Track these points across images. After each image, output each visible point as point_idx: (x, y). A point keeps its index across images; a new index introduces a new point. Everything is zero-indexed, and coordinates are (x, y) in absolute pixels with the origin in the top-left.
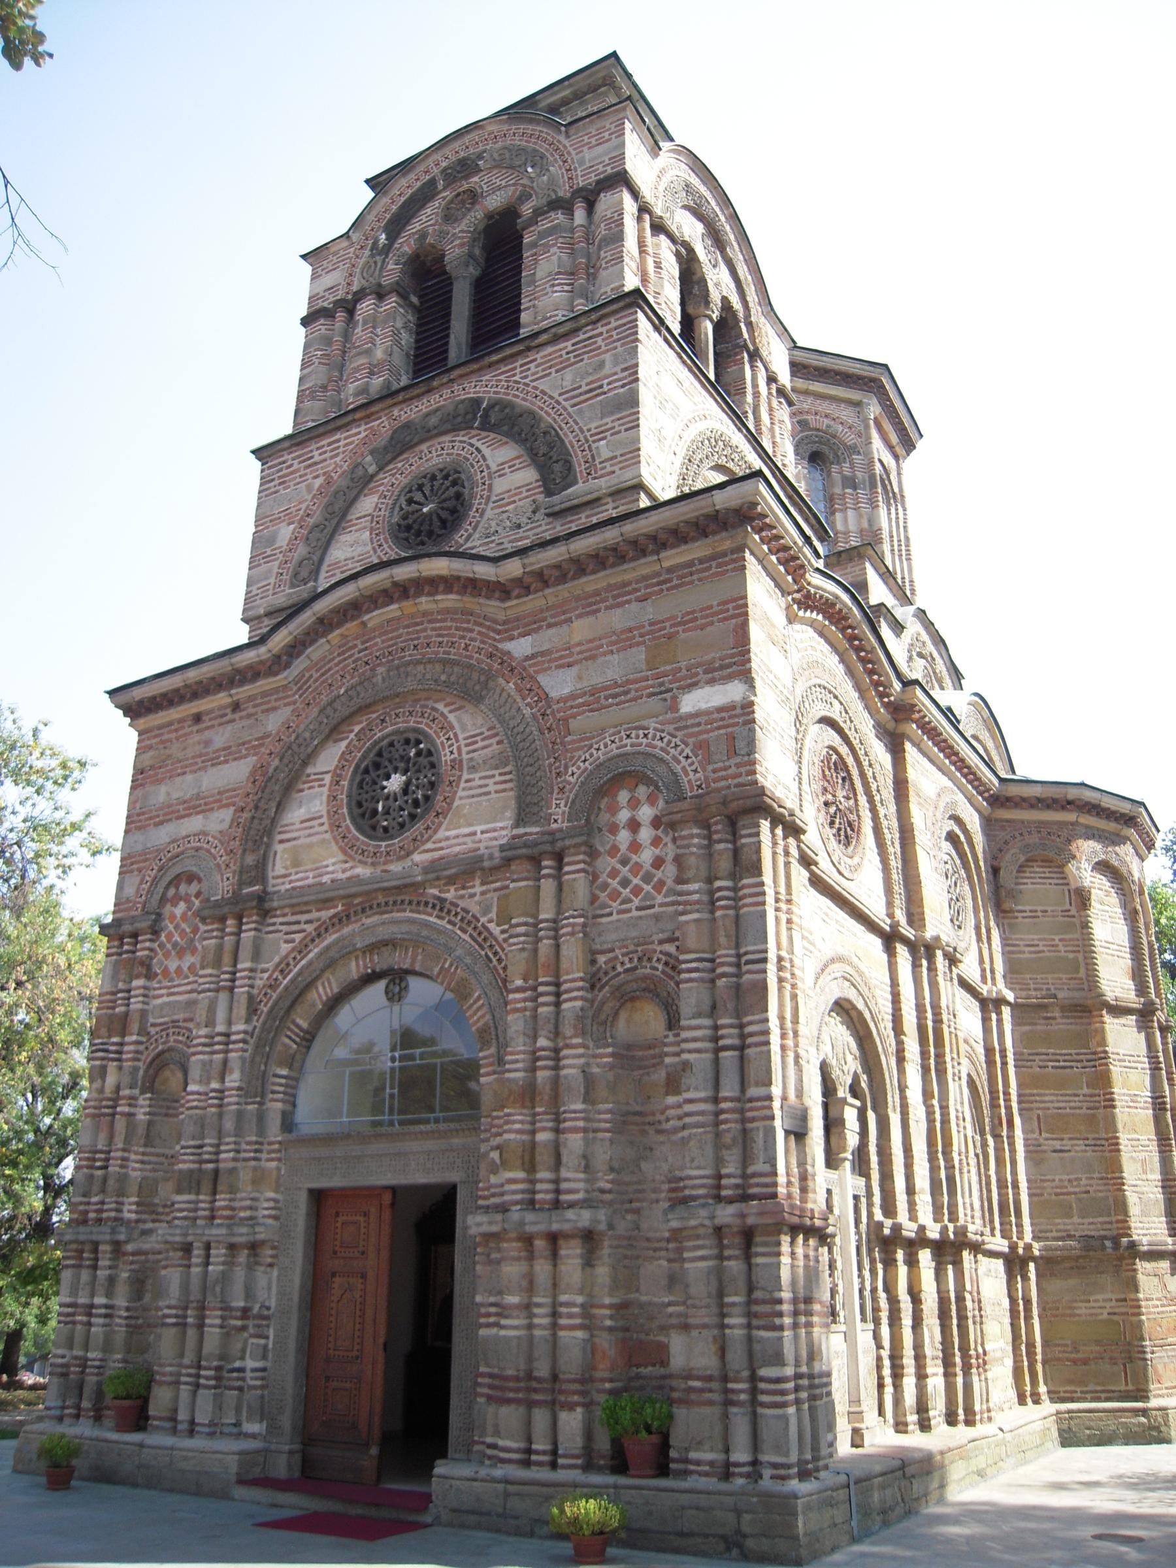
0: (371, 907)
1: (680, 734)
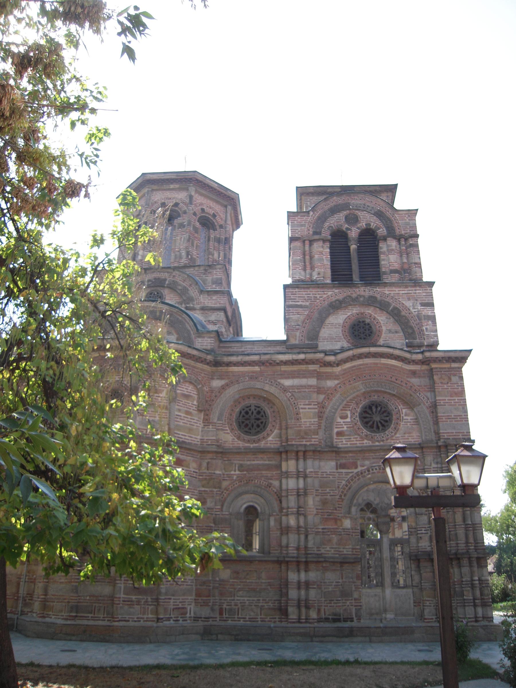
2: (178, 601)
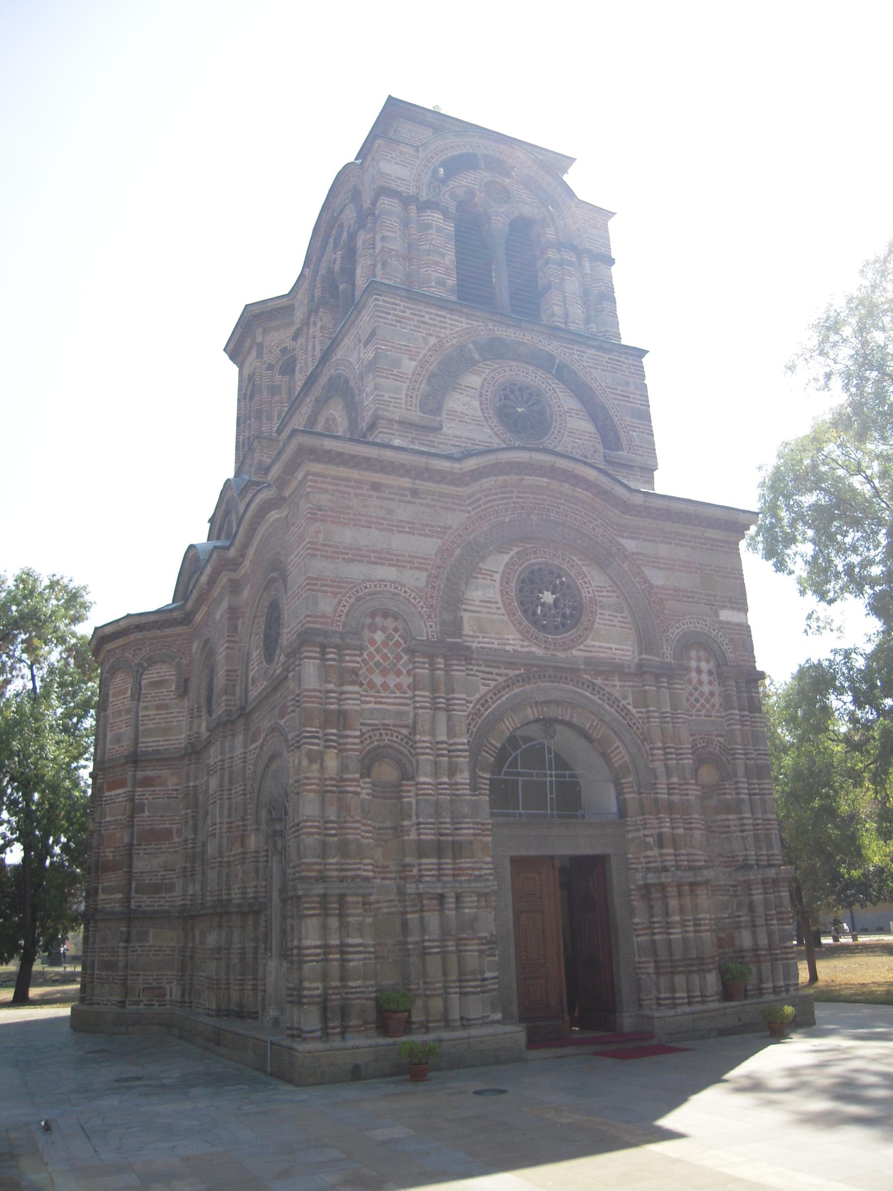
0: (545, 676)
1: (723, 631)
2: (151, 978)
